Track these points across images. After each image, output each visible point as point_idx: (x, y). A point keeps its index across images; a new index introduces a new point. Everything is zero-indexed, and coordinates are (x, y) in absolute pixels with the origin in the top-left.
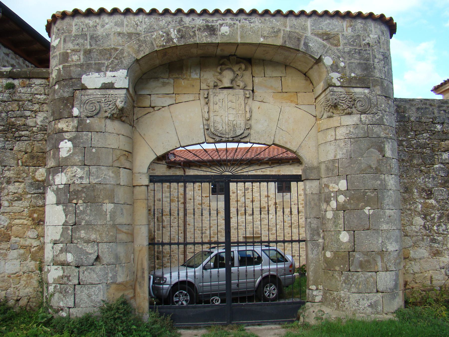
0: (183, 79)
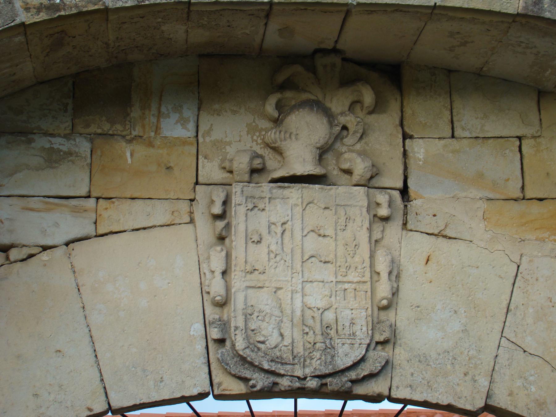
0: (130, 141)
